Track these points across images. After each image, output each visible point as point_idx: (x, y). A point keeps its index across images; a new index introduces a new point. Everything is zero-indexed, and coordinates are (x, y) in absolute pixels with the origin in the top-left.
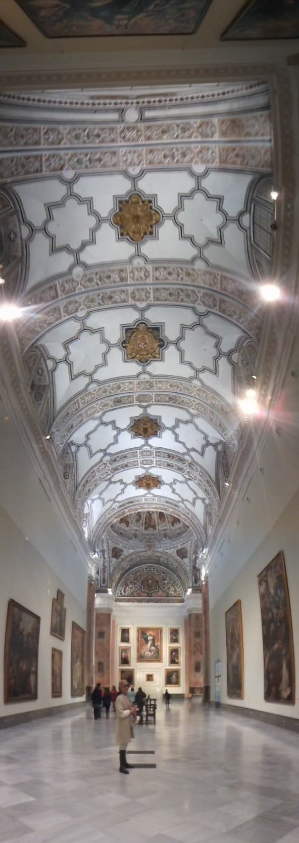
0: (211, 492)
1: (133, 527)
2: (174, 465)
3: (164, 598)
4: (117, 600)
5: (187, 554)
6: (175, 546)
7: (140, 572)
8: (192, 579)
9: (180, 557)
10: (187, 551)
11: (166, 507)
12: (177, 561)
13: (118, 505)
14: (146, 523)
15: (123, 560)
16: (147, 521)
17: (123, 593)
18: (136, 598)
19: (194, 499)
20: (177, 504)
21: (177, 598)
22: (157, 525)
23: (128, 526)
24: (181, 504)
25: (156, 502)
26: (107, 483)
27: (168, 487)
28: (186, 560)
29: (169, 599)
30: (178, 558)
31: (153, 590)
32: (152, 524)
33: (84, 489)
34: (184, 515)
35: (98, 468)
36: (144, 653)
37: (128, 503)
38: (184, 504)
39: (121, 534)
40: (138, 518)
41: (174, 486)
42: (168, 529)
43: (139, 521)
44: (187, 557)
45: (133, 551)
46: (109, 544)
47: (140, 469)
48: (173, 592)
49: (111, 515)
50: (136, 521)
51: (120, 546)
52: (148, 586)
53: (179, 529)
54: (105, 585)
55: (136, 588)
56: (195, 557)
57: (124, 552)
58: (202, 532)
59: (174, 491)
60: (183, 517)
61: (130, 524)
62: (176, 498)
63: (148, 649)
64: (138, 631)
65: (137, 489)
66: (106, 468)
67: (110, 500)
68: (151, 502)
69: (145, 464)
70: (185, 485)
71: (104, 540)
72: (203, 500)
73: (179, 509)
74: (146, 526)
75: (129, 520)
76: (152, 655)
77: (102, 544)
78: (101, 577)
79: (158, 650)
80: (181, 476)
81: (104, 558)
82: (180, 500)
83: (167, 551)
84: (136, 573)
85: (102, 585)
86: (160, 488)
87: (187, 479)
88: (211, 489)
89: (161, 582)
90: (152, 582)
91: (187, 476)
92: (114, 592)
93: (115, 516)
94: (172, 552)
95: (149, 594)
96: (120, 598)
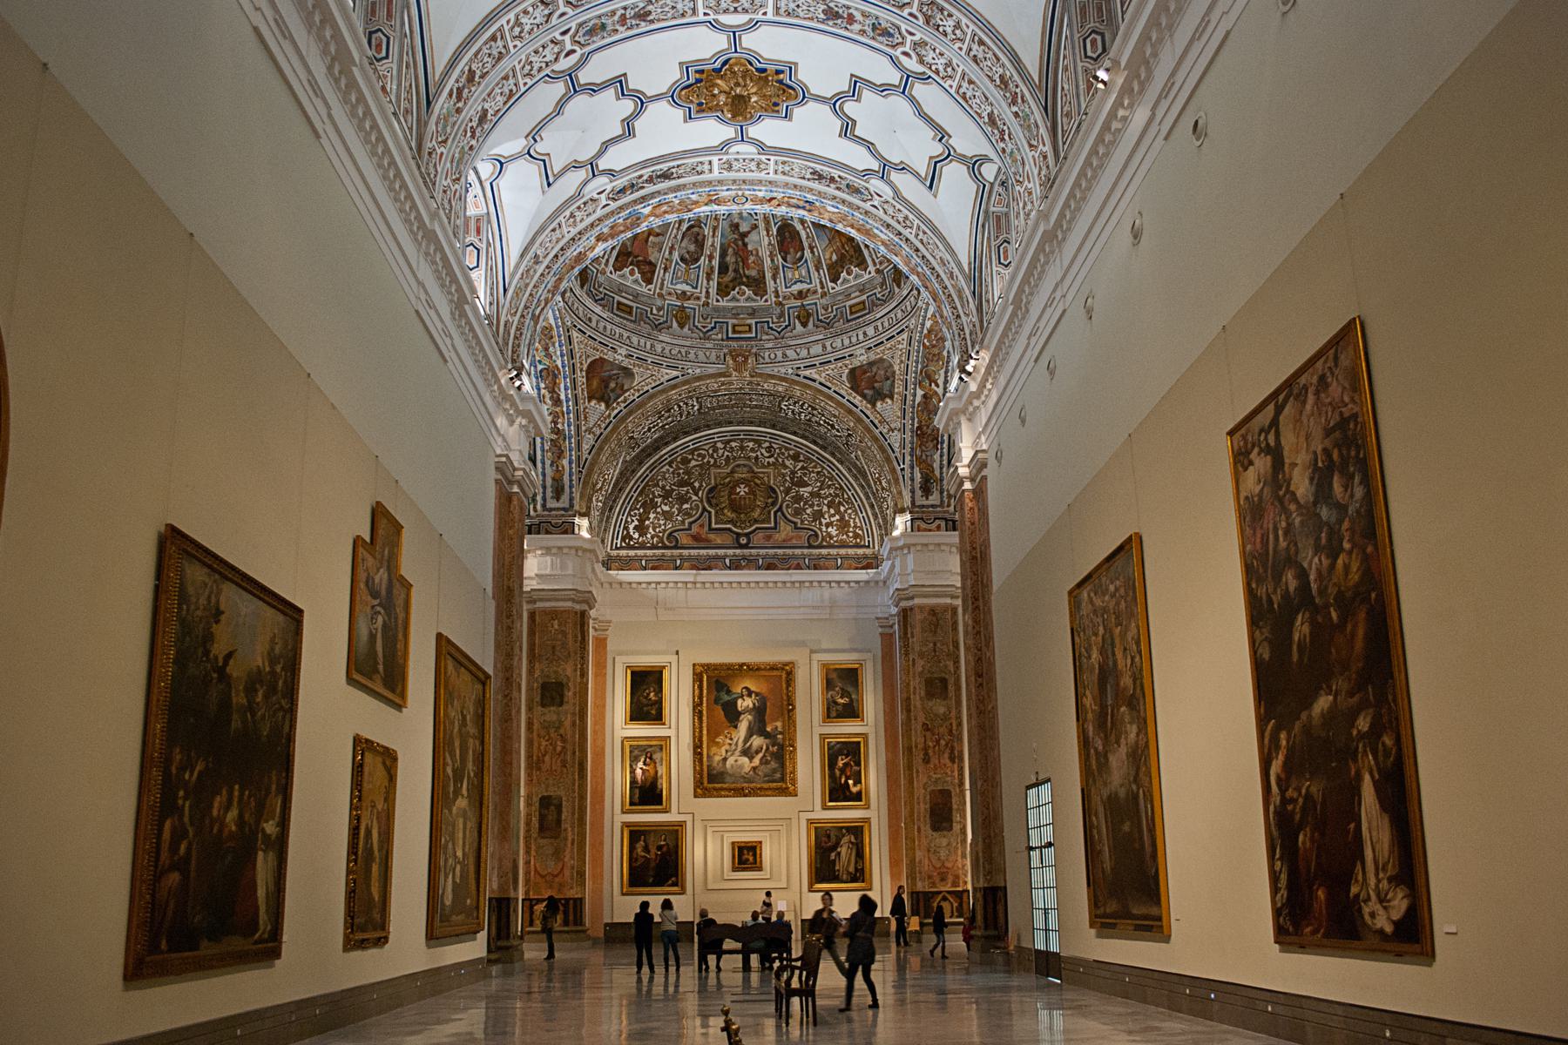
0: (1014, 126)
1: (671, 282)
2: (858, 16)
3: (798, 552)
4: (608, 564)
5: (893, 385)
6: (846, 352)
7: (704, 457)
8: (912, 480)
9: (864, 396)
10: (894, 372)
11: (810, 197)
12: (850, 412)
13: (609, 188)
14: (723, 269)
16: (730, 259)
17: (636, 536)
18: (685, 552)
19: (936, 163)
20: (858, 182)
21: (851, 551)
22: (768, 275)
24: (876, 184)
25: (772, 176)
26: (559, 88)
27: (826, 109)
28: (889, 408)
29: (820, 557)
30: (857, 400)
31: (756, 521)
32: (753, 273)
33: (458, 111)
34: (888, 226)
35: (518, 23)
36: (725, 759)
37: (650, 180)
38: (890, 184)
39: (624, 309)
40: (692, 248)
41: (850, 108)
42: (815, 292)
43: (697, 260)
44: (892, 398)
45: (675, 373)
47: (703, 29)
48: (833, 531)
49: (581, 227)
50: (683, 259)
51: (620, 357)
52: (735, 507)
53: (862, 289)
54: (564, 502)
55: (688, 514)
56: (924, 396)
57: (637, 379)
58: (960, 292)
59: (848, 129)
60: (885, 235)
61: (659, 272)
62: (860, 159)
63: (739, 748)
64: (697, 677)
65: (689, 117)
66: (554, 20)
67: (576, 165)
68: (748, 175)
69: (726, 11)
70: (899, 103)
71: (555, 333)
72: (974, 165)
73: (867, 206)
74: (727, 279)
75: (653, 256)
76: (754, 769)
77: (546, 349)
78: (544, 475)
79: (782, 747)
80: (885, 61)
81: (557, 401)
82: (875, 165)
84: (685, 461)
85: (551, 504)
86: (788, 116)
87: (908, 76)
88: (1016, 115)
89: (787, 491)
90: (752, 492)
91: (912, 64)
92: (598, 530)
93: (596, 231)
94: (835, 377)
95: (738, 535)
96: (623, 553)
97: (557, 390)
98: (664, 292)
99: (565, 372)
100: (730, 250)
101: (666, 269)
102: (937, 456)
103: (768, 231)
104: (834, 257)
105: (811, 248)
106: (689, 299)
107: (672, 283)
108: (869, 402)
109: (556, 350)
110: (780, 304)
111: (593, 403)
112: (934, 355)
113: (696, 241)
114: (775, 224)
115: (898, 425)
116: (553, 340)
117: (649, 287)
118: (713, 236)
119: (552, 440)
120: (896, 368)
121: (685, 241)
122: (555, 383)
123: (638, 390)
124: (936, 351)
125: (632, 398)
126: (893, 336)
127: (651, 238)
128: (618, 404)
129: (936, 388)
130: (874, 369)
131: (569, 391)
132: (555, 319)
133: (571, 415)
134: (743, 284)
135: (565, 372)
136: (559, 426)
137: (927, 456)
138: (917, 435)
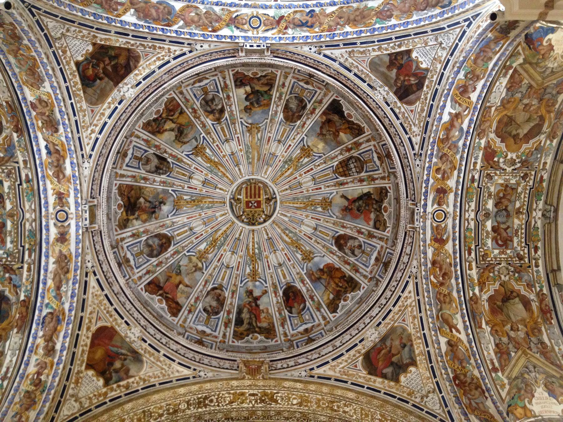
5: (412, 351)
9: (384, 376)
10: (409, 335)
14: (239, 322)
15: (132, 394)
16: (245, 315)
23: (175, 314)
30: (378, 382)
32: (264, 325)
40: (214, 304)
43: (217, 313)
44: (413, 363)
45: (186, 372)
46: (89, 296)
50: (205, 310)
56: (449, 343)
61: (184, 312)
71: (72, 266)
75: (181, 299)
77: (58, 288)
81: (50, 351)
83: (321, 371)
97: (54, 338)
98: (186, 325)
99: (70, 317)
100: (245, 310)
101: (190, 311)
102: (489, 403)
103: (275, 293)
104: (332, 296)
105: (312, 298)
106: (208, 335)
107: (194, 323)
108: (392, 380)
109: (67, 289)
110: (289, 340)
111: (91, 373)
112: (445, 295)
113: (218, 300)
114: (281, 288)
115: (431, 386)
116: (68, 275)
117: (174, 318)
118: (232, 297)
119: (28, 392)
120: (411, 329)
121: (209, 299)
122: (55, 329)
123: (144, 380)
124: (445, 290)
125: (135, 387)
126: (400, 297)
127: (181, 286)
128: (119, 386)
129: (458, 334)
130: (388, 343)
131: (68, 339)
132: (77, 243)
133: (61, 366)
134: (256, 332)
135: (70, 317)
136: (43, 378)
137: (477, 403)
138: (456, 385)
